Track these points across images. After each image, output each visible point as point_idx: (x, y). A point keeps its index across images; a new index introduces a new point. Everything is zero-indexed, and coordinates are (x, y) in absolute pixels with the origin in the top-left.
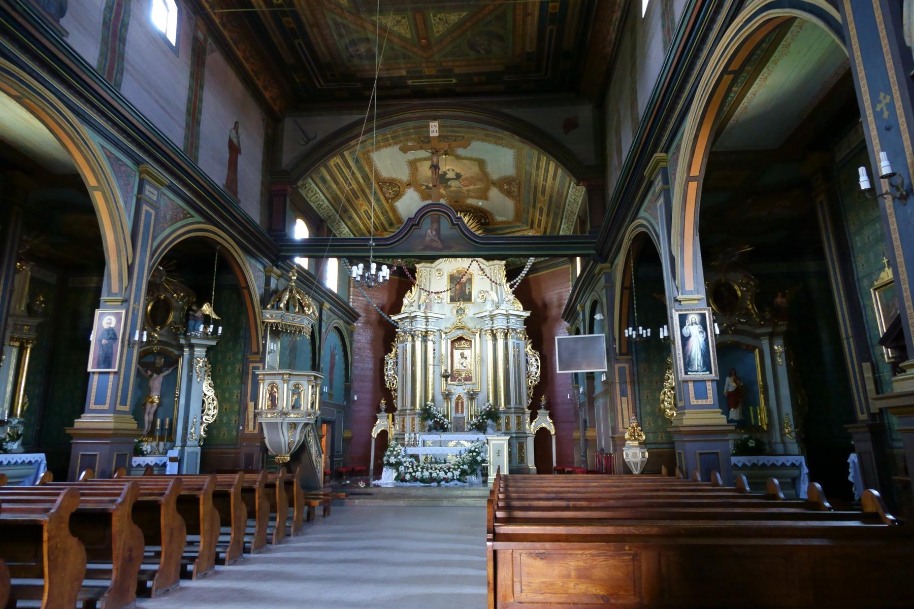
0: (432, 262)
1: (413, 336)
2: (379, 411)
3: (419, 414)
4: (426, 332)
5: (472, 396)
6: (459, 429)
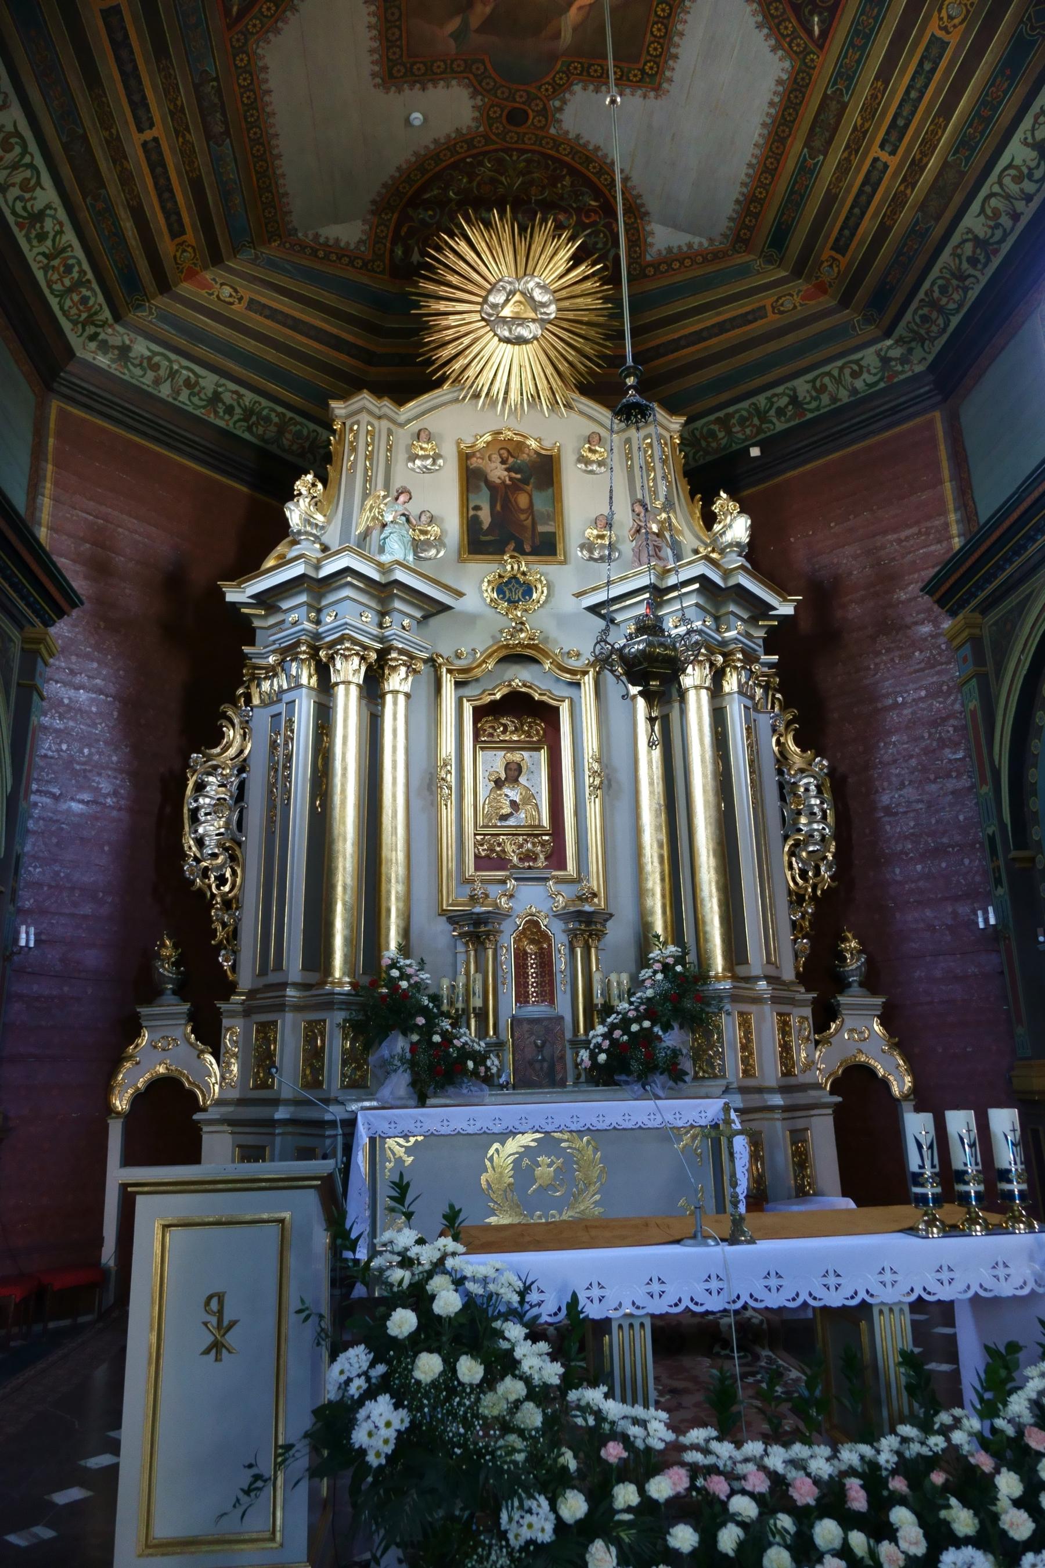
0: (401, 402)
1: (323, 671)
2: (151, 993)
3: (346, 1004)
4: (383, 654)
5: (587, 924)
6: (541, 1068)
